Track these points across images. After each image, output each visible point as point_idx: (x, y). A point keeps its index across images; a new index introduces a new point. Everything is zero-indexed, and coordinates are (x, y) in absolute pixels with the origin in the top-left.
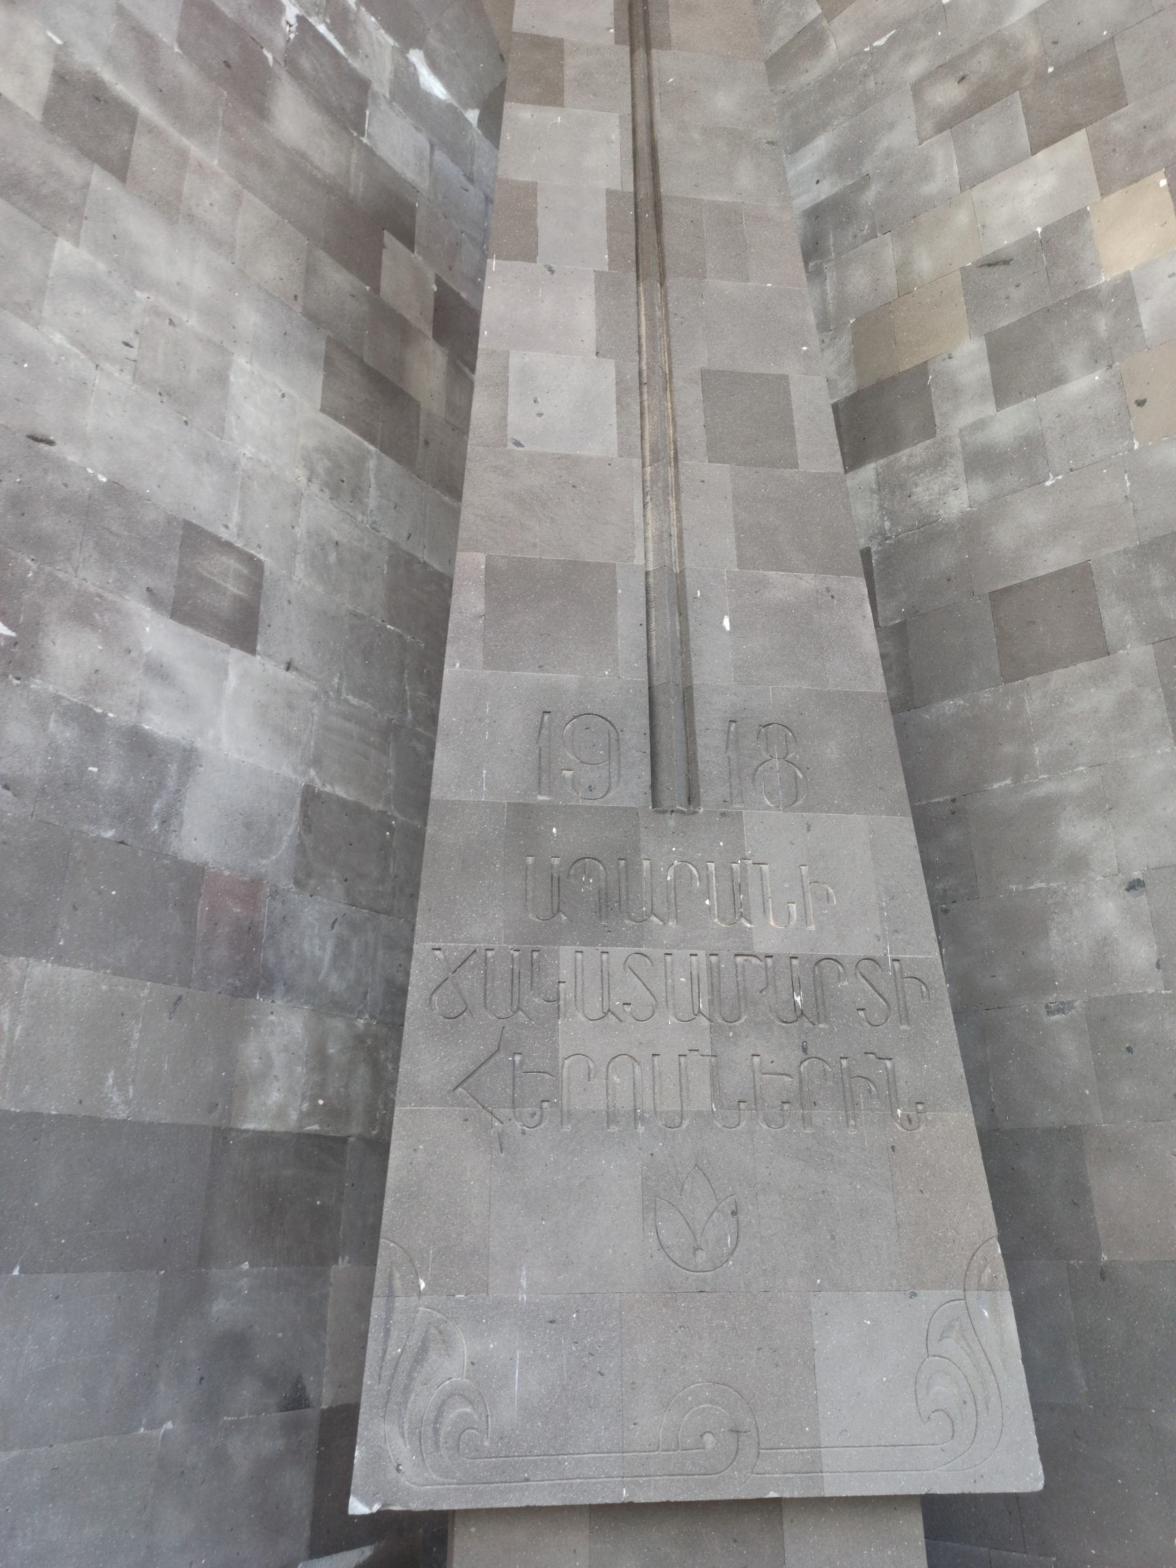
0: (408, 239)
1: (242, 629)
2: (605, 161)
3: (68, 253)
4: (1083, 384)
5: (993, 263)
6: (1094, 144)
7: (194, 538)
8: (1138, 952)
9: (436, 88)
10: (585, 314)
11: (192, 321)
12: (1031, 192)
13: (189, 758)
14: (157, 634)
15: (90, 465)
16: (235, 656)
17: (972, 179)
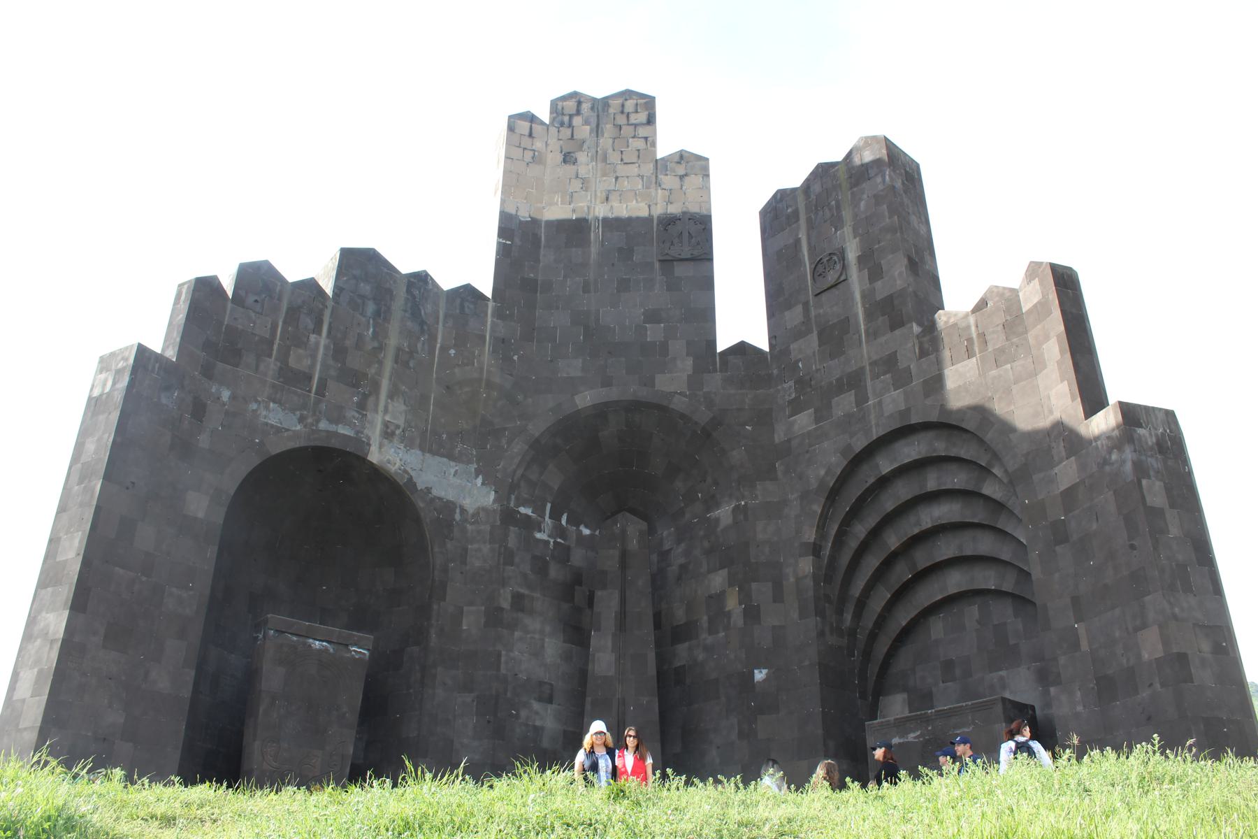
0: (580, 584)
1: (550, 700)
2: (615, 603)
3: (517, 634)
4: (722, 634)
5: (710, 597)
6: (729, 573)
7: (541, 683)
8: (717, 761)
9: (586, 532)
10: (610, 644)
11: (537, 636)
12: (718, 580)
13: (542, 728)
14: (536, 706)
15: (523, 676)
16: (551, 708)
17: (709, 572)
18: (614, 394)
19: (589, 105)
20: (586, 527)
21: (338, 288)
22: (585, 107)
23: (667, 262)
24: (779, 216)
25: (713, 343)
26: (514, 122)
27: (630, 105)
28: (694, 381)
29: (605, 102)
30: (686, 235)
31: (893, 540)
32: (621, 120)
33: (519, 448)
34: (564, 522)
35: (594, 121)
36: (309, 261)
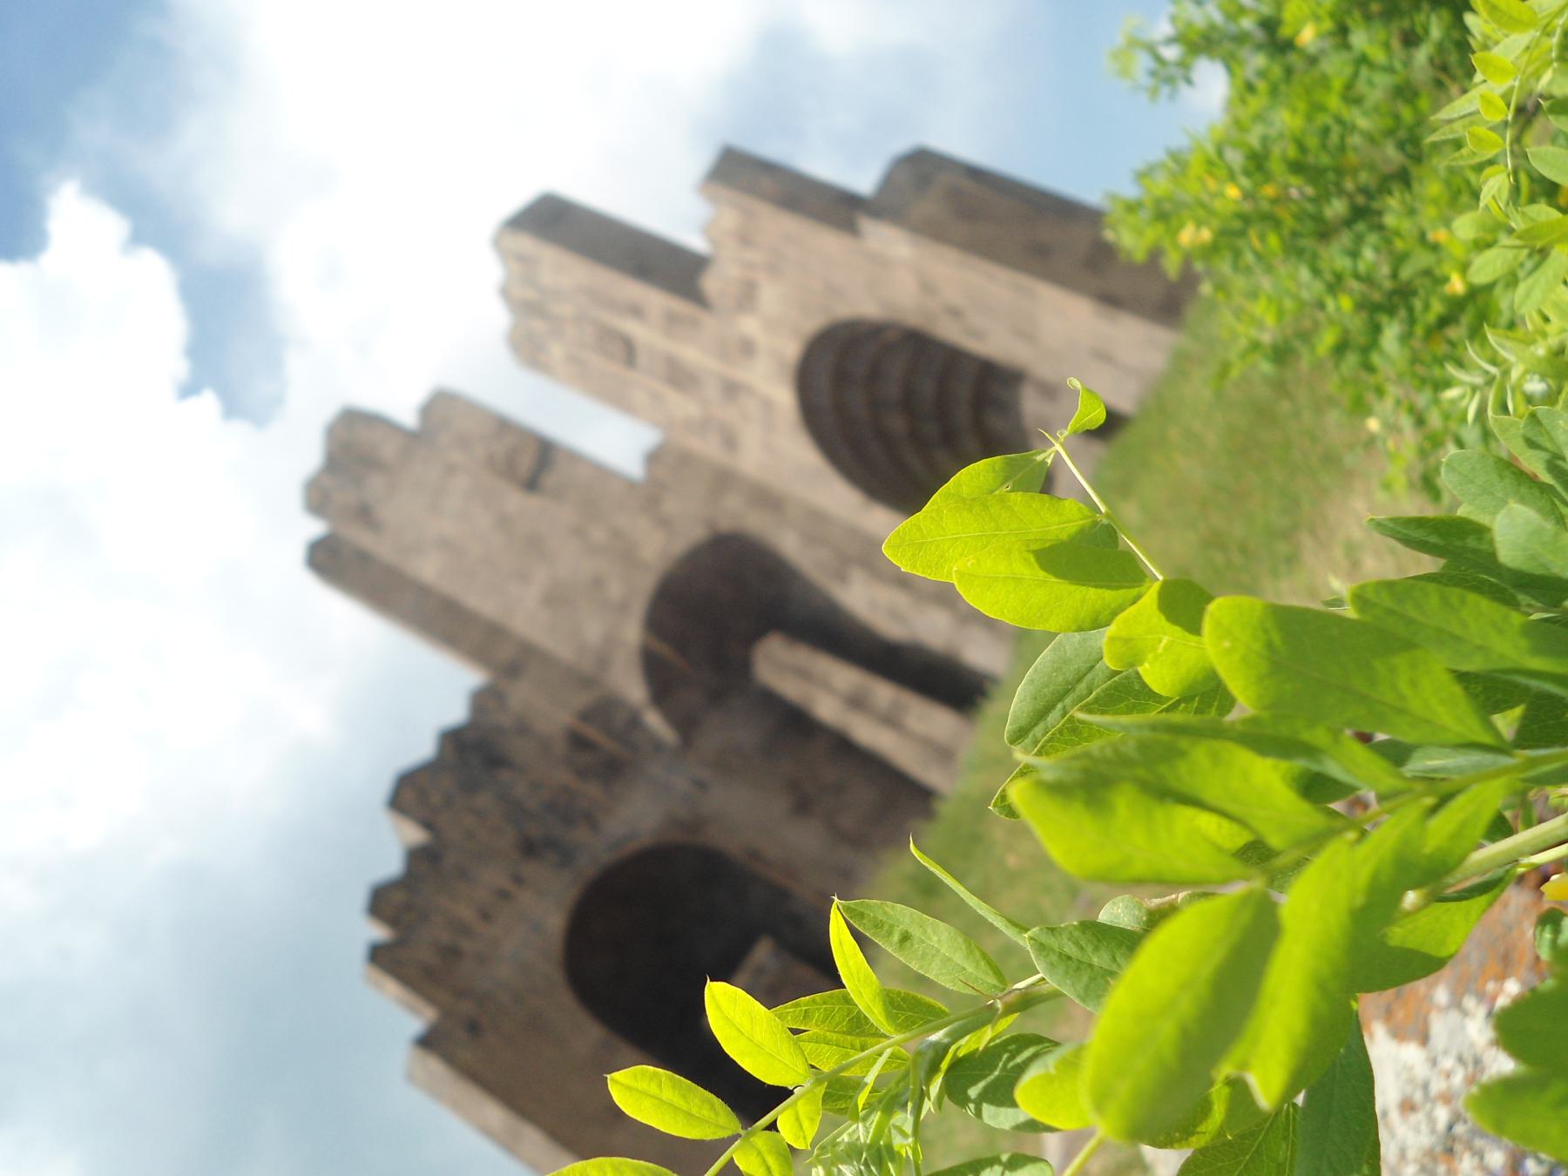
21: (427, 825)
23: (531, 484)
24: (528, 349)
28: (664, 523)
31: (897, 424)
33: (654, 721)
36: (387, 847)
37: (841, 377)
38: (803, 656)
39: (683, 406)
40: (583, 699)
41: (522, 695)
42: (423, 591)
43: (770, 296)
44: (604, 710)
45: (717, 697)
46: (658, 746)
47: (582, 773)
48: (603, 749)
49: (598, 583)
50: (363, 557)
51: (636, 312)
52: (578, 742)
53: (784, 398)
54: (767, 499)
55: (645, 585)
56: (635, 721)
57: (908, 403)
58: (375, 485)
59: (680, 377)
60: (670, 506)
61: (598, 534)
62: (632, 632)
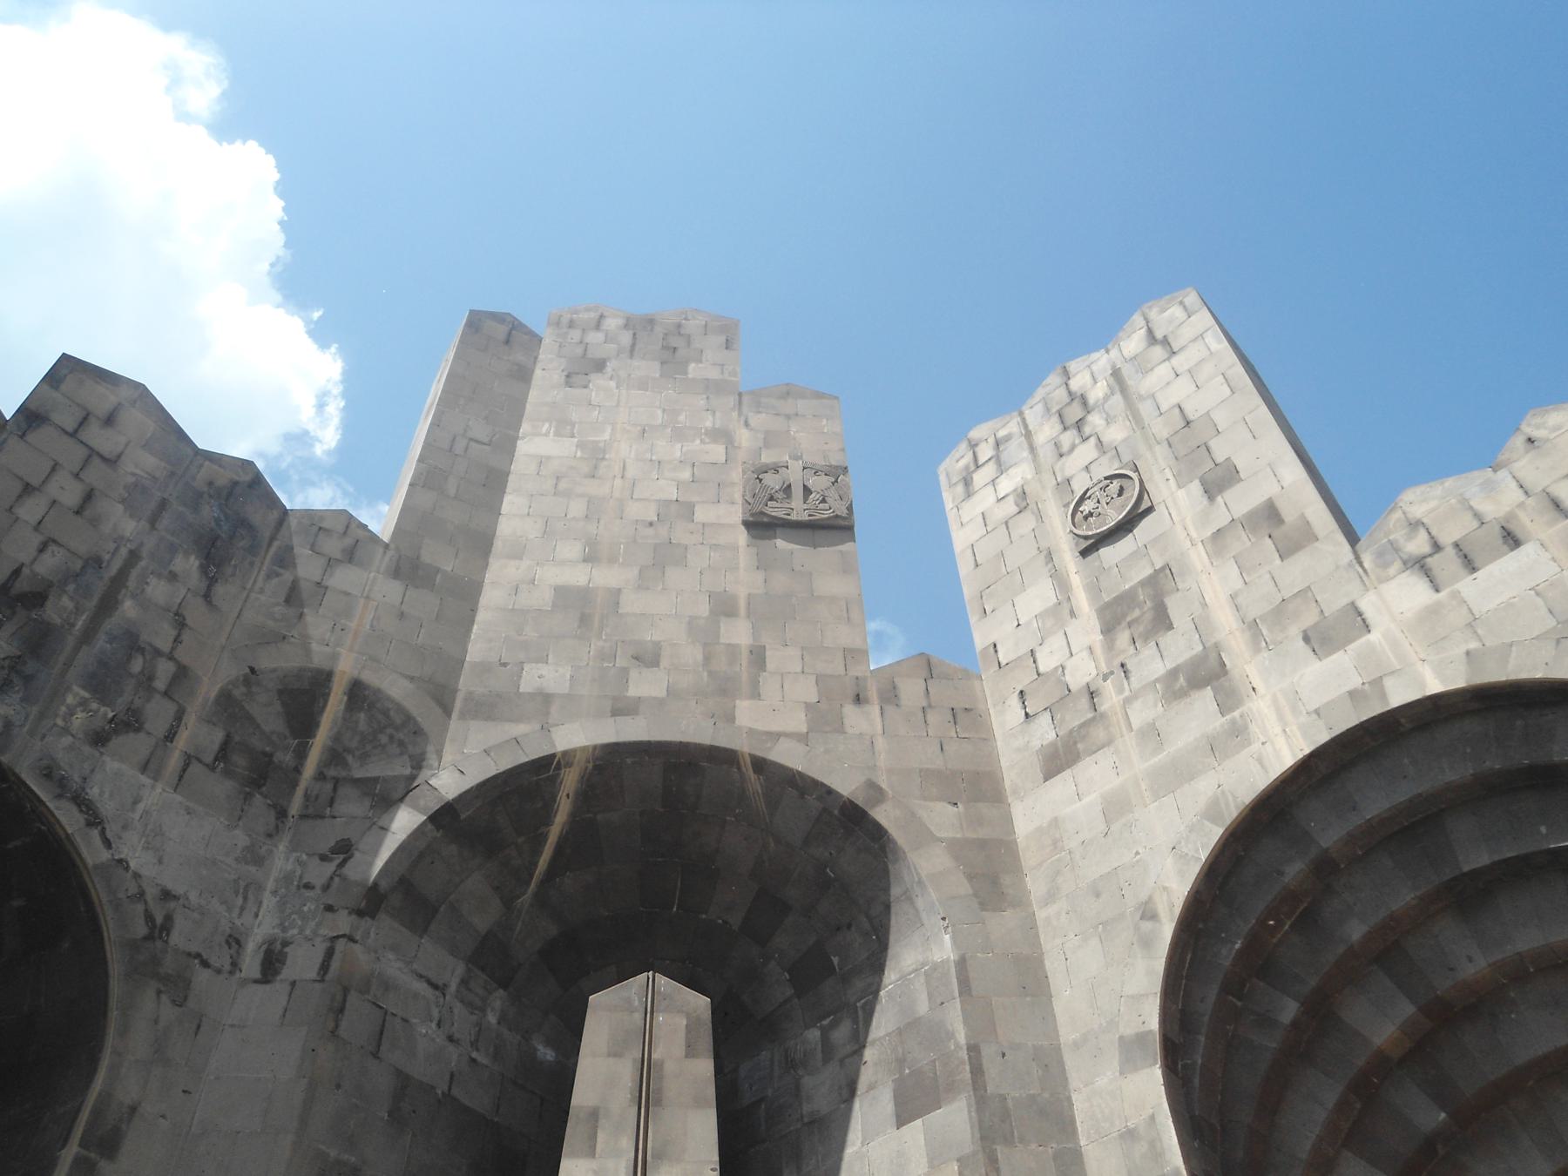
9: (547, 1054)
18: (634, 730)
19: (621, 322)
20: (549, 1043)
22: (612, 323)
23: (761, 526)
25: (854, 655)
26: (476, 322)
27: (693, 326)
28: (824, 719)
29: (650, 322)
30: (798, 492)
31: (1380, 1021)
32: (675, 341)
33: (405, 821)
34: (492, 1018)
35: (626, 338)
37: (1414, 828)
38: (691, 1075)
39: (1077, 652)
40: (395, 687)
41: (371, 593)
42: (506, 445)
43: (1502, 582)
44: (388, 735)
45: (491, 959)
46: (344, 849)
47: (228, 706)
48: (298, 742)
49: (648, 658)
50: (523, 375)
51: (1218, 482)
52: (303, 697)
53: (1280, 746)
54: (992, 872)
55: (690, 726)
56: (385, 799)
57: (1448, 1017)
58: (647, 368)
59: (1141, 612)
60: (863, 721)
61: (738, 633)
62: (576, 735)
